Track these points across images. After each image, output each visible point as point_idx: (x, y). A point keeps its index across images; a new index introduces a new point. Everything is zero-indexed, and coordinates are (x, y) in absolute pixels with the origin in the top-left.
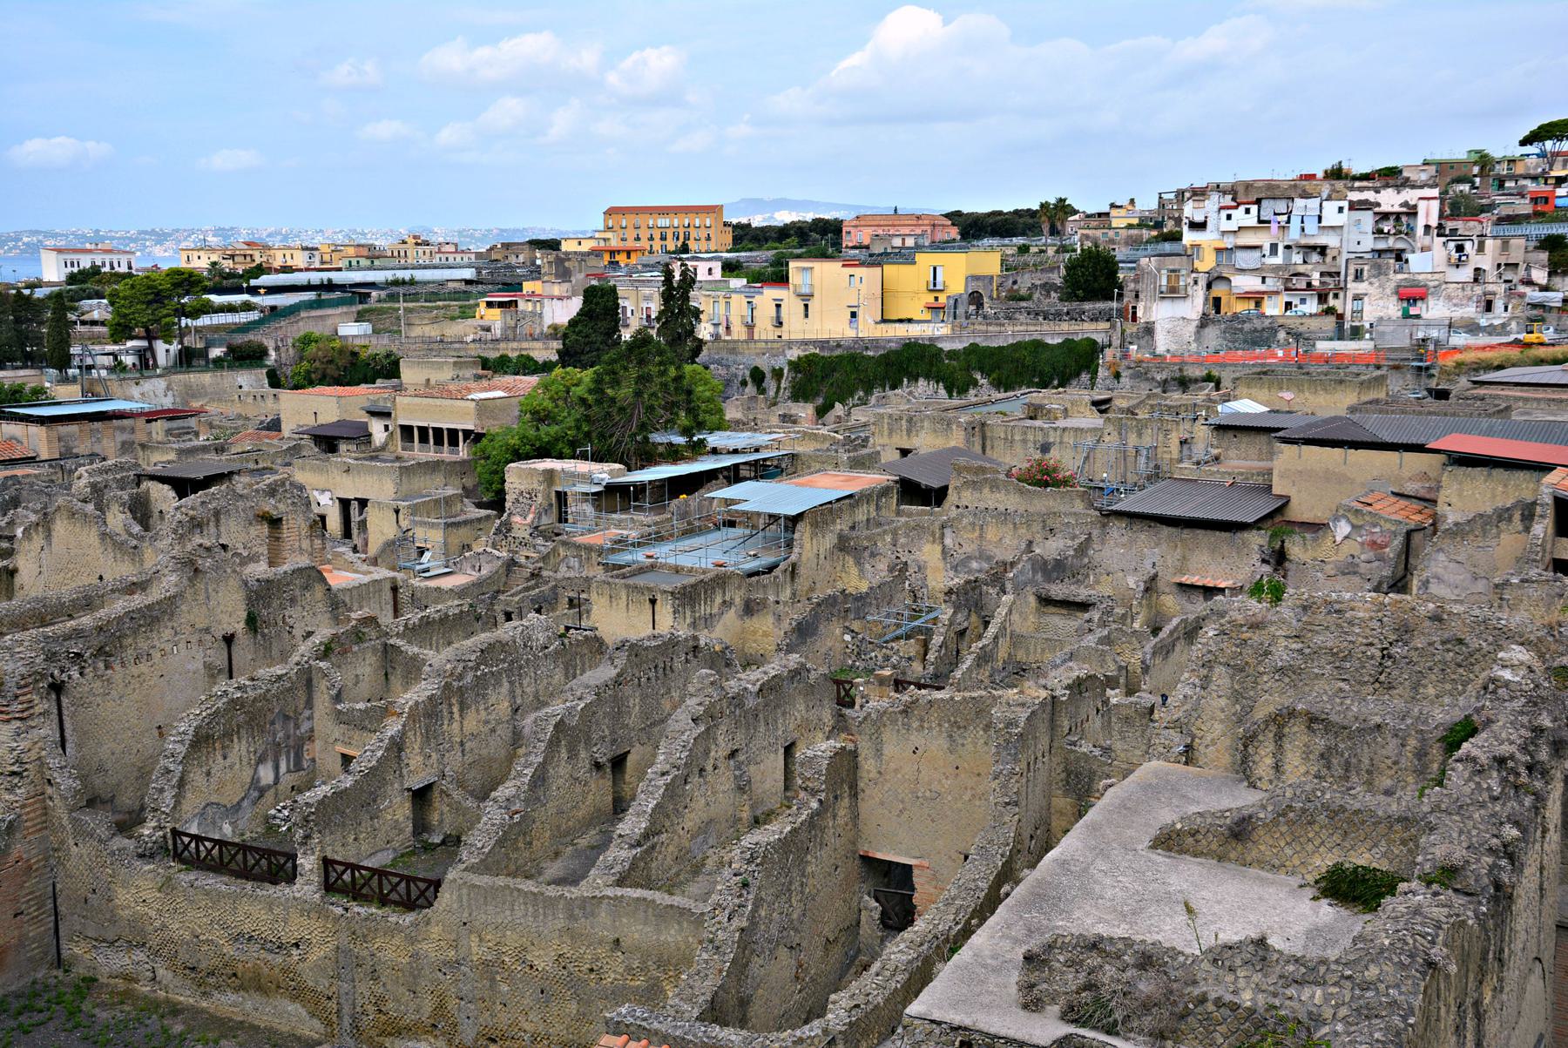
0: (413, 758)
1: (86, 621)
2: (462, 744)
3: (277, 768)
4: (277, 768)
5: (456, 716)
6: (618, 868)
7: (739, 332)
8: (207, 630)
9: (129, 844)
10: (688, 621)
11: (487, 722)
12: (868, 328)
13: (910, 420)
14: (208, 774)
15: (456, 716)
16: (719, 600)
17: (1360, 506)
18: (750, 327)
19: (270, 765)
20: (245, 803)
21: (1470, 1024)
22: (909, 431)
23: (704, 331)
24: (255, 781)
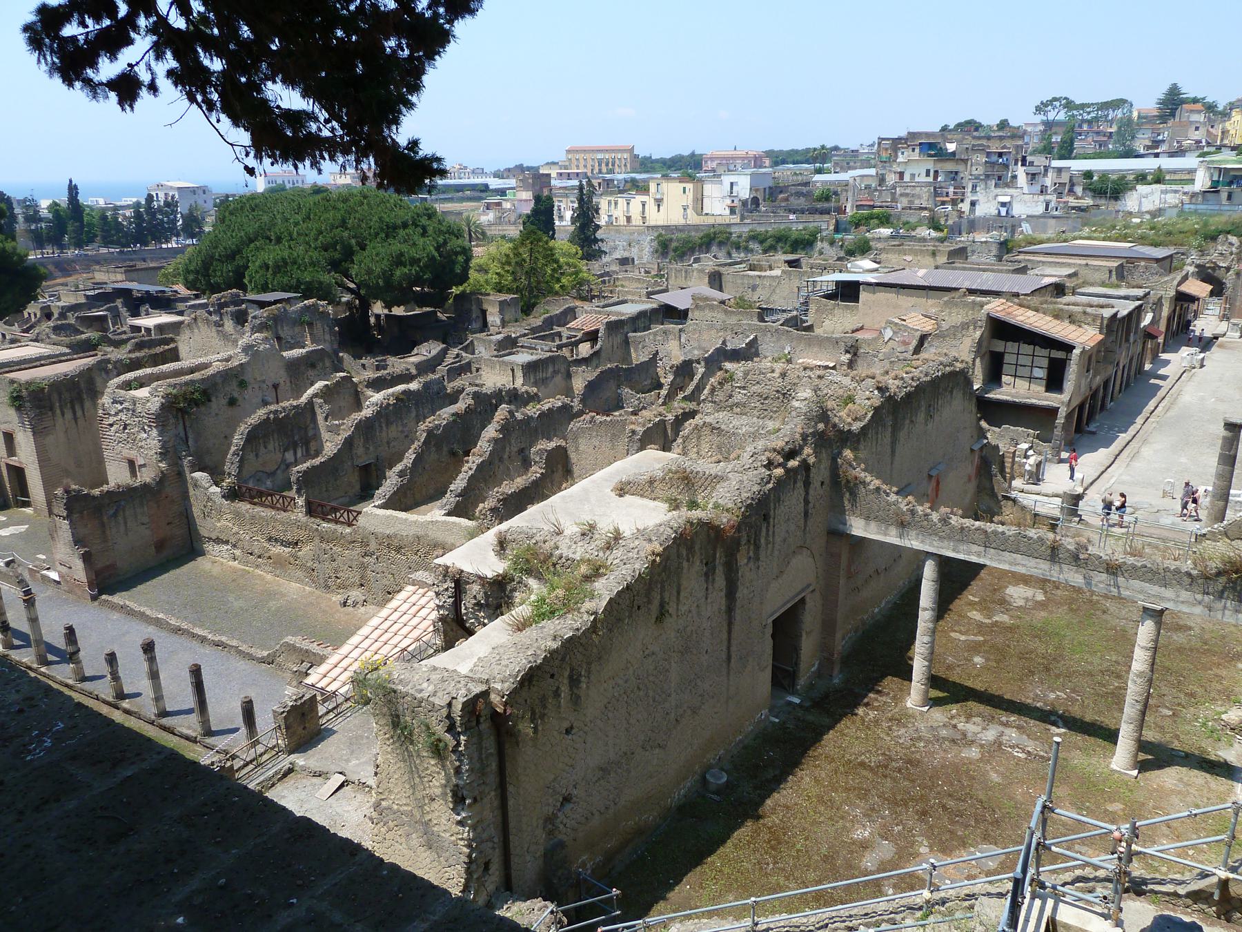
0: (360, 450)
1: (197, 376)
2: (388, 443)
3: (295, 453)
4: (295, 453)
5: (384, 428)
6: (447, 507)
7: (622, 221)
8: (264, 382)
9: (218, 490)
10: (532, 380)
11: (402, 432)
12: (693, 219)
13: (686, 272)
14: (257, 455)
15: (384, 428)
16: (551, 370)
17: (897, 321)
18: (629, 219)
19: (291, 452)
20: (279, 472)
21: (720, 571)
22: (686, 277)
23: (602, 220)
24: (283, 460)
